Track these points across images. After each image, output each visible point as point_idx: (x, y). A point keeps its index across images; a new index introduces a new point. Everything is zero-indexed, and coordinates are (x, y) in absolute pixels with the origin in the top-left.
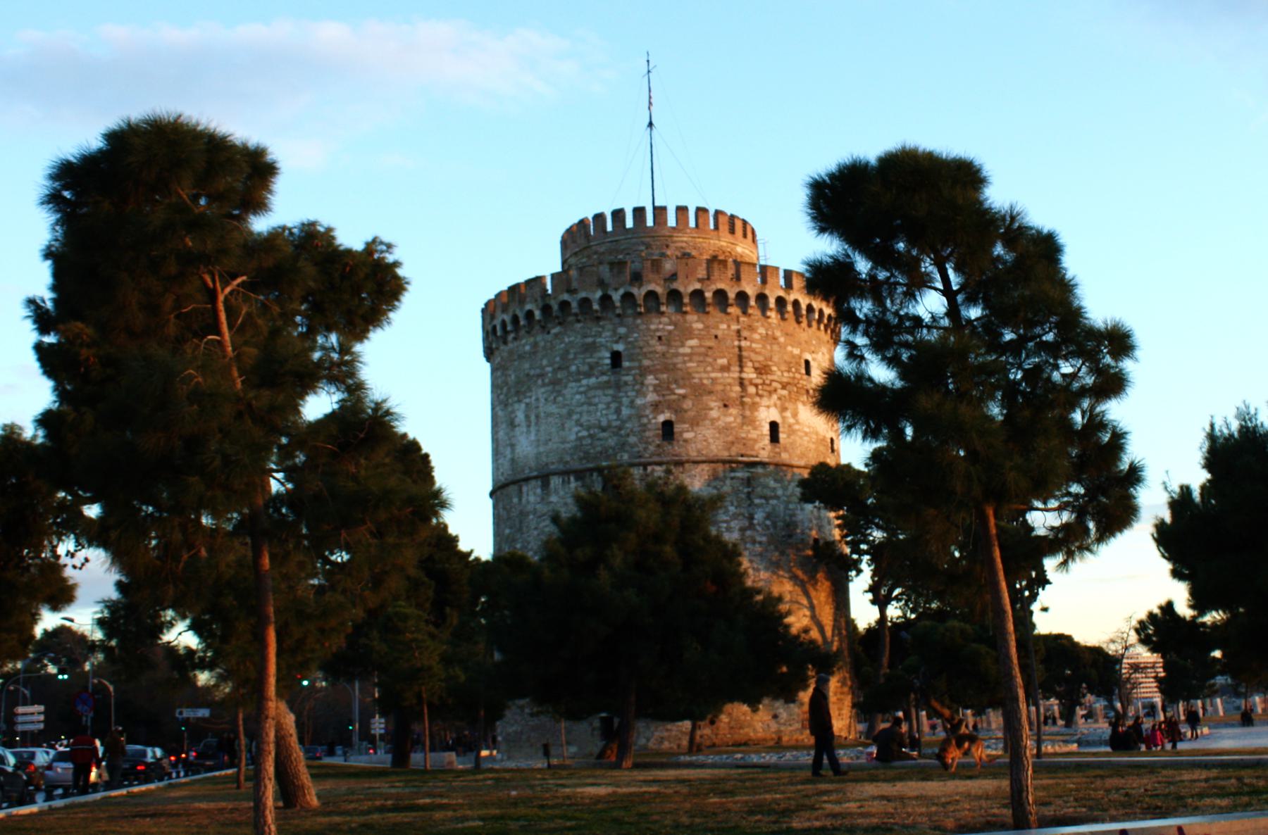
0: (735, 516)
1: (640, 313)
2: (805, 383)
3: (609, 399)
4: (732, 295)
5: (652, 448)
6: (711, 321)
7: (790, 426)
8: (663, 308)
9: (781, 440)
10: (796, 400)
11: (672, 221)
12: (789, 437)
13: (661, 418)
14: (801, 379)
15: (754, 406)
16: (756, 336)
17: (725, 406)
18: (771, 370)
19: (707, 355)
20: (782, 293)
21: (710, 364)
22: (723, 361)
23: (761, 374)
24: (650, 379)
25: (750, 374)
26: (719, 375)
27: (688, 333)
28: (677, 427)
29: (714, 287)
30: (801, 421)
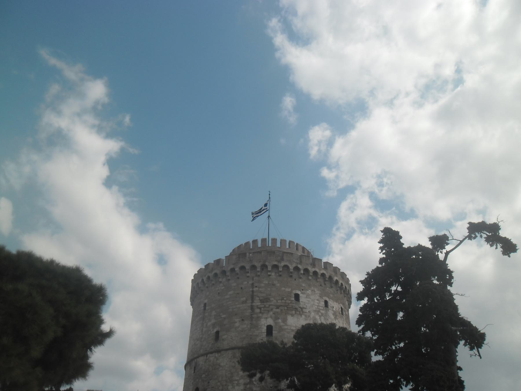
1: (213, 284)
2: (294, 305)
4: (248, 267)
7: (280, 327)
9: (274, 335)
13: (215, 330)
14: (291, 303)
15: (259, 318)
16: (263, 285)
17: (243, 320)
18: (270, 300)
20: (276, 263)
22: (244, 299)
23: (264, 302)
25: (257, 303)
26: (241, 305)
28: (220, 334)
29: (240, 265)
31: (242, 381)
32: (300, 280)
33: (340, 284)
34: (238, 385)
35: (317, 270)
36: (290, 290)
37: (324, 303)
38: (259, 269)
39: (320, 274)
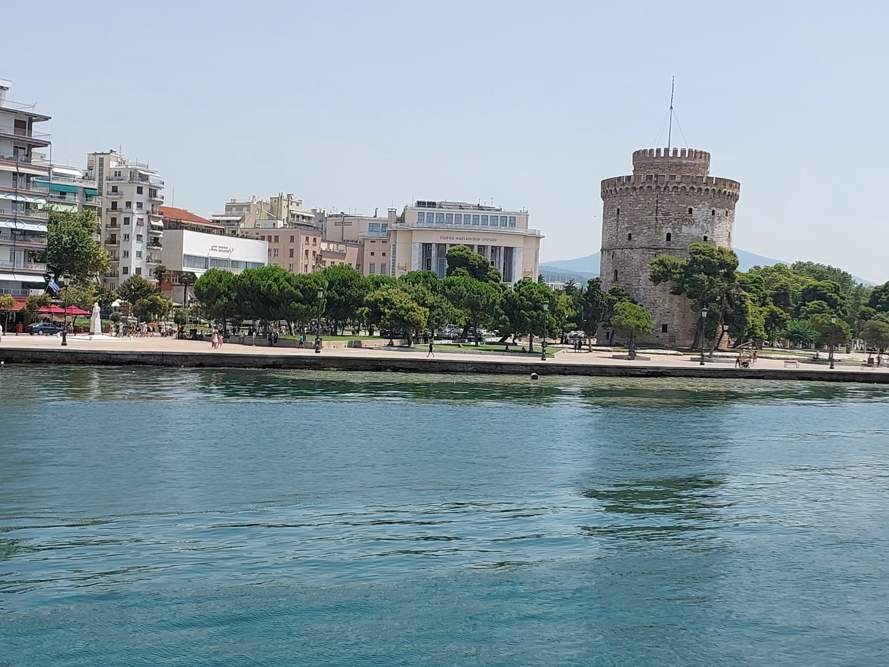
0: (649, 267)
3: (615, 225)
4: (653, 188)
7: (677, 234)
8: (631, 194)
10: (681, 224)
12: (675, 238)
13: (628, 233)
15: (661, 228)
19: (644, 210)
20: (676, 185)
21: (645, 213)
24: (626, 219)
25: (660, 216)
27: (639, 202)
28: (632, 236)
29: (647, 185)
31: (649, 270)
32: (694, 197)
33: (727, 193)
34: (646, 272)
35: (709, 187)
36: (685, 205)
37: (711, 213)
38: (662, 190)
39: (710, 190)
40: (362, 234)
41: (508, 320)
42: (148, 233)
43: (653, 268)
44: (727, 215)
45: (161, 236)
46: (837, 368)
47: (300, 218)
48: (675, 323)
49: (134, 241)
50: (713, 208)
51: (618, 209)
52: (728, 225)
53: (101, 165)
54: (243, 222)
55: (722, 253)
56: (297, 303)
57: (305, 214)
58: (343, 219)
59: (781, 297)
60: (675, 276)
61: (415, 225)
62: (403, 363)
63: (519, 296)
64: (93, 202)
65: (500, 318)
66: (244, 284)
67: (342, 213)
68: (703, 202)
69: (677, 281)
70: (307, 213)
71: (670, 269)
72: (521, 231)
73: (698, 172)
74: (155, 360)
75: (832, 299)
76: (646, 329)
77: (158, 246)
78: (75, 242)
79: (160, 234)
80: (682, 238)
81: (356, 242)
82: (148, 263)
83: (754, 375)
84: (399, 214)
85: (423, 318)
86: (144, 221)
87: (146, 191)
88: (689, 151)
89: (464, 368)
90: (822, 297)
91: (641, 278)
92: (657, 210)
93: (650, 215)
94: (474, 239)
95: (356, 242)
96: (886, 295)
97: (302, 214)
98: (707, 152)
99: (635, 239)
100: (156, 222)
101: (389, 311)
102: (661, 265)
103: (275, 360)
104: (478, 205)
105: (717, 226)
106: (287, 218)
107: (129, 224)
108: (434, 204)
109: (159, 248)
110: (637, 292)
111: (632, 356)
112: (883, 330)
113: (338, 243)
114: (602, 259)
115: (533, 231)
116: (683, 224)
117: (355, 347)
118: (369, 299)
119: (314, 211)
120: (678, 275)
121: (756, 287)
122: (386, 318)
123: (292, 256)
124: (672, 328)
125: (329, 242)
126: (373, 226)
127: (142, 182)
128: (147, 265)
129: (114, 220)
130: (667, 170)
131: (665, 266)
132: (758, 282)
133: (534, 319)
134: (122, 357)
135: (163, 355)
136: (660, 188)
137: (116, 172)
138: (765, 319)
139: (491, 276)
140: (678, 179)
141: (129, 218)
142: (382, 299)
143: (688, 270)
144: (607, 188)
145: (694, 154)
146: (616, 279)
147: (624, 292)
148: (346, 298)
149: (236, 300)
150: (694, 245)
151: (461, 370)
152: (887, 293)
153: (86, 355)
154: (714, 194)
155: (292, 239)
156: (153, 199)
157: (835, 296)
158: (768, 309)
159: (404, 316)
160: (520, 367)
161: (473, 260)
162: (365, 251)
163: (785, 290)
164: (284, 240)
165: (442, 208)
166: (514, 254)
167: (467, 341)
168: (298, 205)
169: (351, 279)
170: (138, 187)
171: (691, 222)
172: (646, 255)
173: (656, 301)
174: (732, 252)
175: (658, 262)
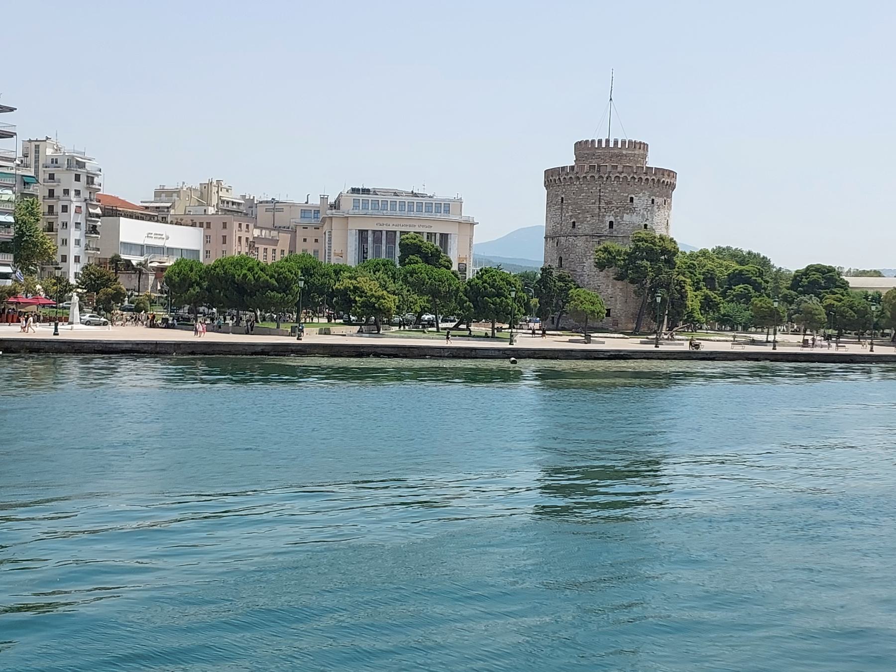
0: (592, 254)
4: (596, 177)
5: (569, 231)
6: (590, 187)
7: (619, 222)
8: (575, 183)
11: (596, 146)
13: (572, 221)
15: (604, 216)
16: (607, 191)
20: (618, 175)
24: (570, 208)
25: (603, 205)
27: (582, 191)
28: (576, 224)
29: (590, 175)
30: (624, 219)
32: (635, 186)
34: (590, 259)
35: (649, 177)
37: (651, 202)
38: (605, 179)
40: (294, 220)
41: (472, 306)
42: (87, 220)
43: (598, 255)
44: (665, 204)
45: (99, 223)
46: (779, 349)
47: (230, 204)
48: (618, 308)
49: (73, 229)
50: (652, 197)
51: (562, 198)
52: (667, 214)
53: (37, 152)
54: (173, 209)
55: (663, 240)
56: (272, 291)
57: (234, 200)
58: (274, 206)
59: (710, 280)
60: (619, 263)
61: (351, 212)
62: (383, 349)
63: (483, 283)
64: (31, 189)
65: (465, 305)
66: (218, 274)
67: (273, 199)
68: (644, 191)
69: (621, 267)
70: (236, 199)
71: (615, 256)
72: (457, 218)
73: (638, 162)
74: (149, 349)
75: (757, 283)
76: (600, 313)
77: (96, 234)
78: (22, 231)
79: (98, 221)
80: (624, 226)
81: (288, 228)
82: (86, 251)
83: (706, 356)
84: (331, 200)
85: (393, 305)
86: (82, 208)
87: (83, 179)
88: (629, 142)
89: (441, 353)
90: (747, 281)
91: (585, 264)
92: (600, 199)
93: (594, 203)
94: (410, 226)
95: (288, 228)
96: (807, 279)
97: (232, 200)
98: (646, 143)
99: (579, 227)
100: (94, 209)
101: (360, 299)
102: (605, 252)
103: (264, 347)
104: (412, 192)
105: (656, 214)
106: (217, 204)
107: (67, 212)
108: (368, 190)
109: (97, 236)
110: (581, 278)
111: (588, 340)
112: (817, 312)
113: (270, 230)
114: (546, 246)
115: (467, 218)
116: (623, 213)
117: (325, 334)
118: (339, 287)
119: (243, 197)
120: (622, 262)
121: (690, 272)
122: (358, 306)
123: (224, 242)
124: (615, 312)
125: (262, 228)
126: (305, 212)
127: (79, 170)
128: (85, 253)
129: (51, 208)
130: (608, 160)
131: (610, 253)
132: (691, 268)
133: (498, 306)
134: (118, 346)
135: (156, 343)
136: (603, 178)
137: (52, 159)
138: (700, 302)
139: (442, 263)
140: (620, 169)
141: (67, 206)
142: (352, 288)
143: (631, 257)
144: (551, 178)
145: (634, 145)
146: (561, 266)
147: (571, 278)
148: (308, 286)
149: (207, 289)
150: (636, 233)
151: (438, 355)
152: (808, 276)
153: (83, 345)
154: (654, 183)
155: (225, 225)
156: (91, 186)
157: (759, 280)
158: (703, 294)
159: (375, 303)
160: (493, 351)
161: (426, 247)
162: (297, 237)
163: (711, 274)
164: (216, 226)
165: (377, 195)
166: (449, 240)
167: (421, 327)
168: (227, 191)
169: (314, 268)
170: (76, 175)
171: (632, 211)
172: (589, 242)
173: (599, 286)
174: (673, 239)
175: (602, 249)
